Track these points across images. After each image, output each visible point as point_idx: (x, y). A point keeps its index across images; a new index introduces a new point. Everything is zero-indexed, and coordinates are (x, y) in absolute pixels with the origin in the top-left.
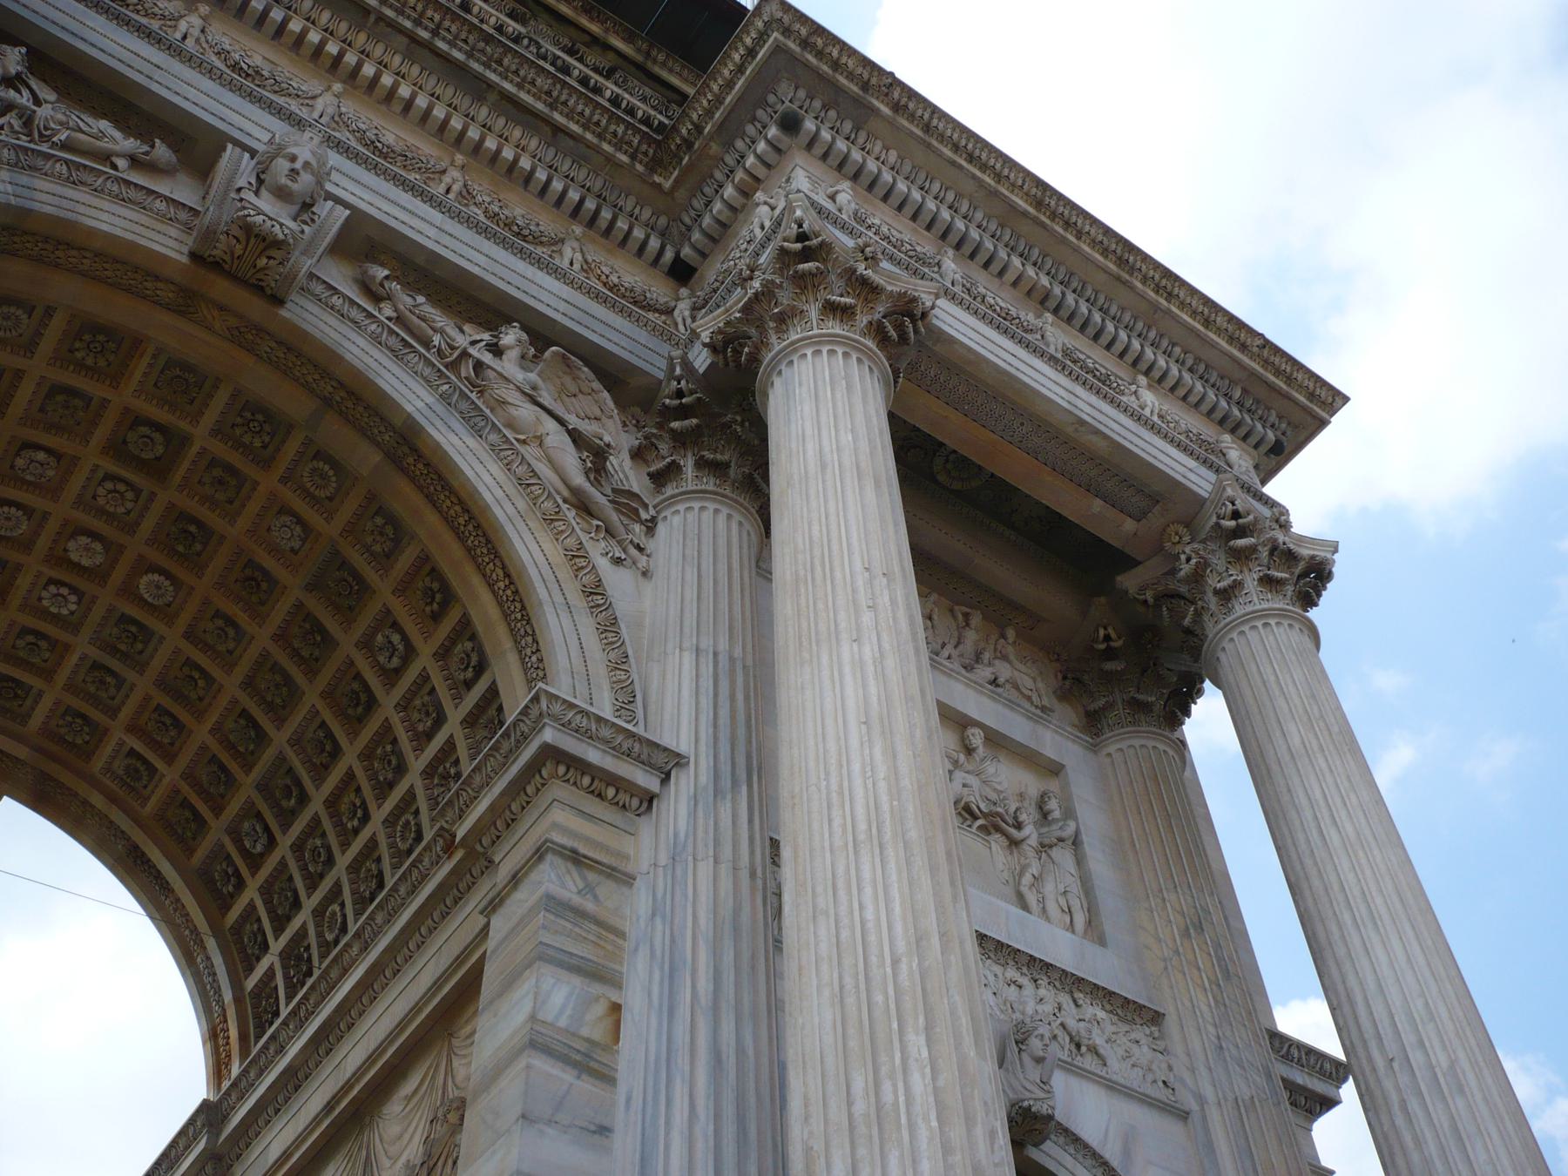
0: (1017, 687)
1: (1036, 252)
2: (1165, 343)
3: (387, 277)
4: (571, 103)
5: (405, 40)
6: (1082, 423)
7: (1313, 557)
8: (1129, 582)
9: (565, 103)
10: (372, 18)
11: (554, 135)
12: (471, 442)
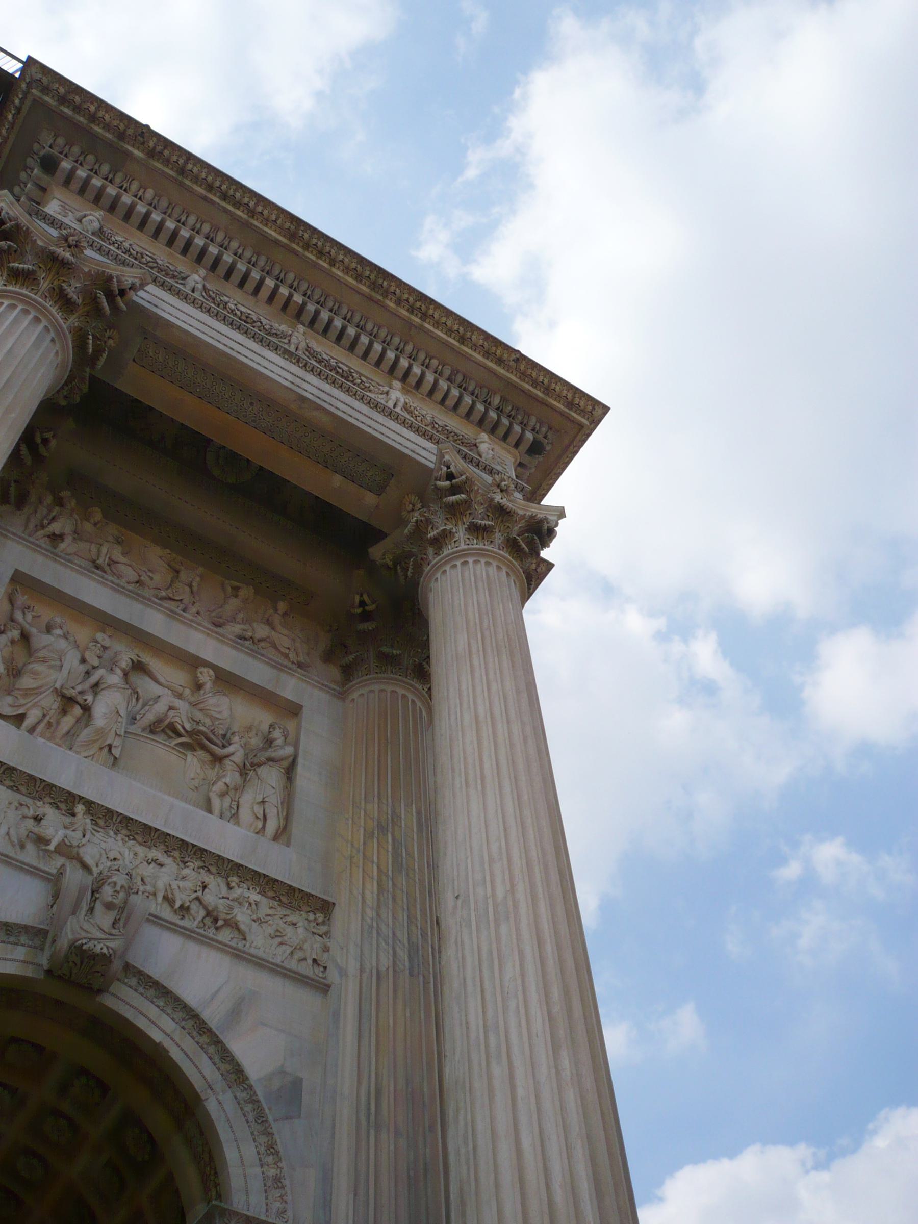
0: (275, 646)
1: (291, 276)
2: (422, 356)
6: (303, 399)
7: (532, 517)
8: (378, 552)
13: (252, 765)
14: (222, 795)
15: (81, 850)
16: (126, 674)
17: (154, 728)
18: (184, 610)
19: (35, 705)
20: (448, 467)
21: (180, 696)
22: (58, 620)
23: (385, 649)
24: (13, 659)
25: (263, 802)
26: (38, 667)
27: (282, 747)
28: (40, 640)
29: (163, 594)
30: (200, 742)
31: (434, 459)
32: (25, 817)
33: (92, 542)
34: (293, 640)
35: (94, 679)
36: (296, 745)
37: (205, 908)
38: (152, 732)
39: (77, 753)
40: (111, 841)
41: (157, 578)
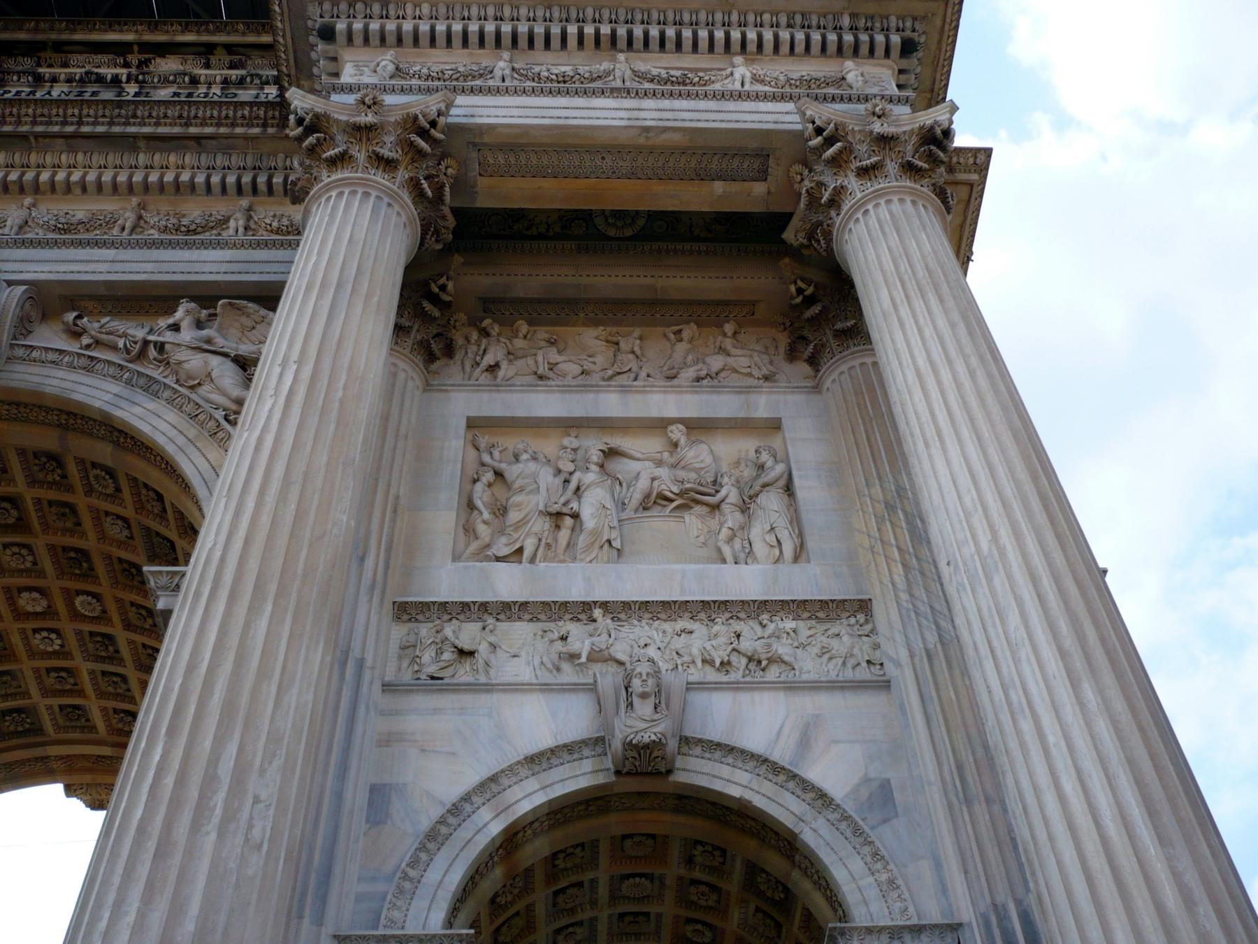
1: (590, 11)
2: (751, 18)
3: (76, 318)
4: (200, 114)
5: (61, 141)
6: (647, 129)
7: (921, 128)
8: (789, 235)
9: (196, 117)
10: (32, 140)
11: (199, 144)
12: (151, 405)
13: (751, 497)
14: (730, 540)
15: (611, 651)
16: (602, 466)
17: (645, 505)
18: (636, 379)
19: (528, 535)
20: (814, 123)
21: (659, 463)
22: (521, 446)
23: (839, 326)
24: (496, 500)
25: (772, 529)
26: (517, 499)
27: (772, 468)
28: (512, 471)
29: (610, 372)
30: (695, 498)
31: (797, 118)
32: (552, 641)
33: (525, 357)
34: (751, 356)
35: (573, 485)
36: (787, 461)
37: (744, 655)
38: (645, 509)
39: (581, 560)
40: (637, 630)
41: (599, 359)
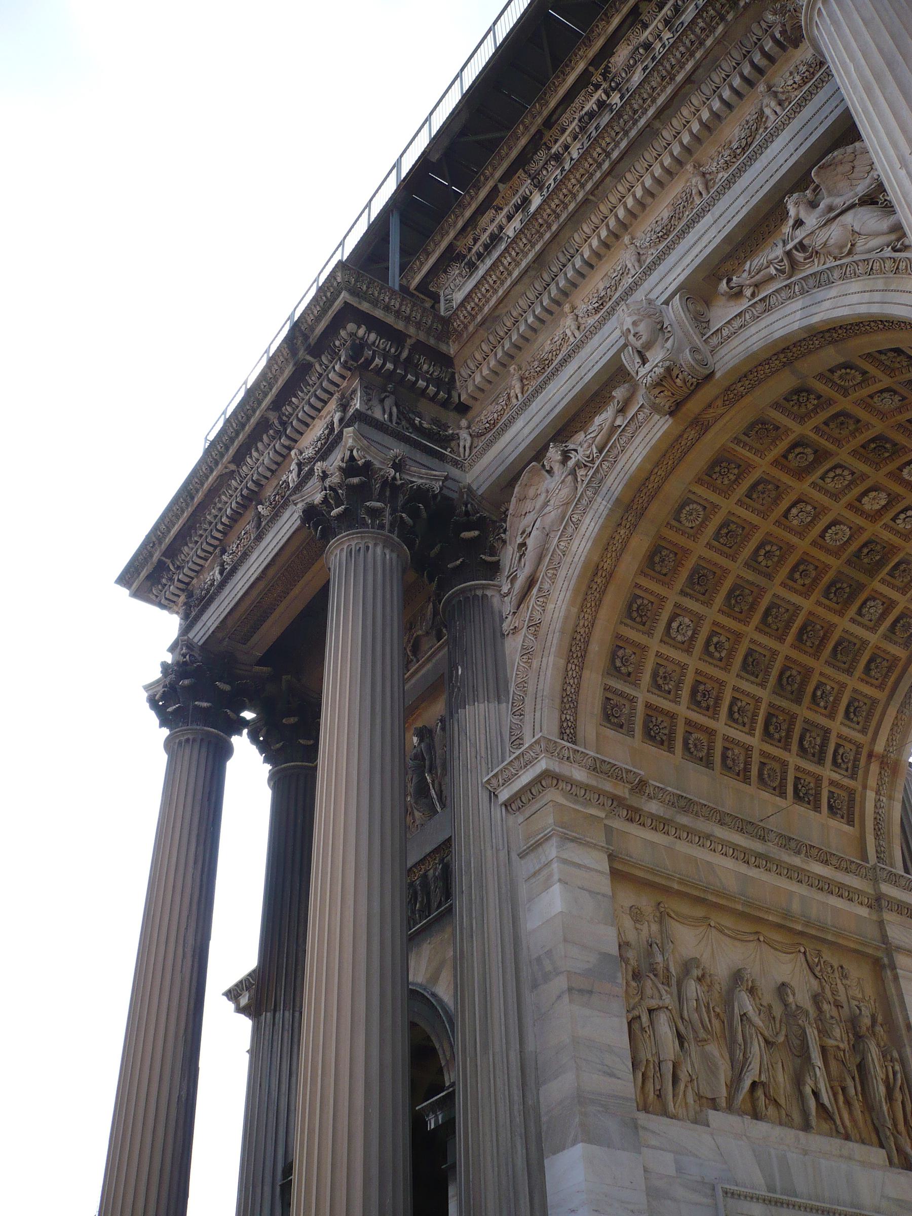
3: (727, 283)
4: (673, 62)
5: (608, 179)
9: (672, 67)
10: (591, 197)
11: (693, 82)
12: (833, 292)
